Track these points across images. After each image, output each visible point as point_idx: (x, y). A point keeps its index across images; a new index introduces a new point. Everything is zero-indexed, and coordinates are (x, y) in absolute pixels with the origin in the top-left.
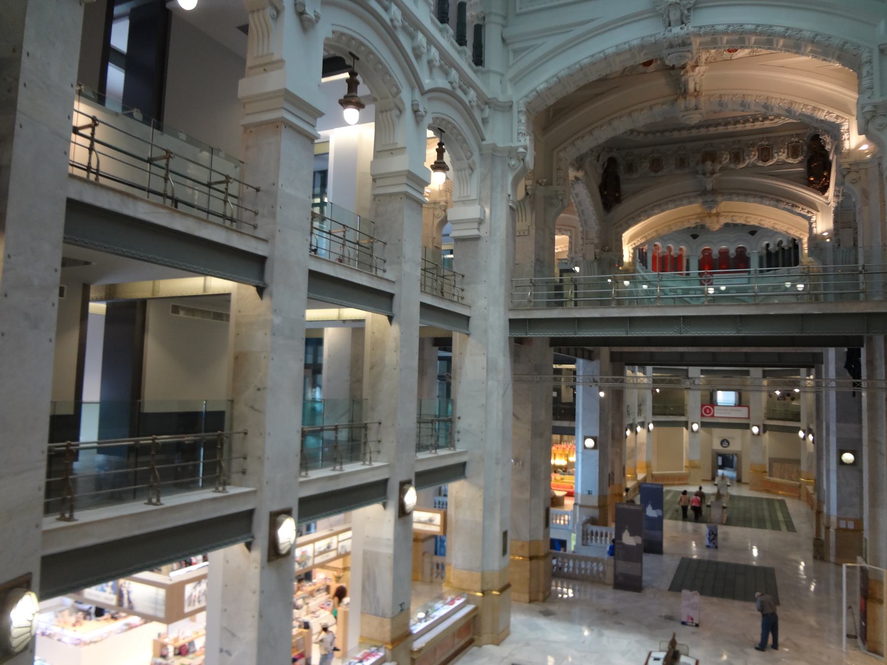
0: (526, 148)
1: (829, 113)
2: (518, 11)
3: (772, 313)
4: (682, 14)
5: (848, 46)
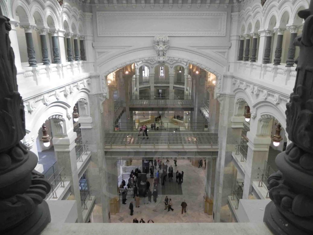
2: (99, 35)
4: (164, 53)
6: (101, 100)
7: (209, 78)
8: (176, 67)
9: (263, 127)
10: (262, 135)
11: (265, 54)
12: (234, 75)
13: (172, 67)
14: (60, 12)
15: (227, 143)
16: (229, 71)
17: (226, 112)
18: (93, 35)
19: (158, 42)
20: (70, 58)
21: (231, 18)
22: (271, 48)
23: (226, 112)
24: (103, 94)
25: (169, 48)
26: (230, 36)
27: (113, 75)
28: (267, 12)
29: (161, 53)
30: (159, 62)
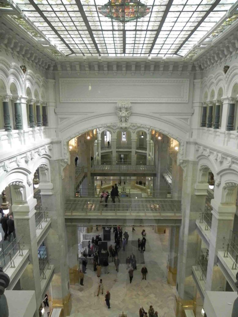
0: (67, 159)
3: (150, 218)
4: (126, 119)
6: (63, 166)
7: (172, 144)
8: (138, 132)
9: (227, 195)
10: (227, 204)
11: (228, 122)
12: (198, 141)
13: (134, 132)
14: (23, 79)
15: (191, 210)
16: (193, 137)
17: (190, 179)
18: (55, 101)
19: (120, 108)
20: (32, 124)
21: (194, 85)
22: (235, 115)
23: (190, 179)
24: (64, 160)
25: (132, 114)
26: (193, 103)
27: (75, 140)
28: (229, 79)
29: (123, 119)
30: (121, 128)
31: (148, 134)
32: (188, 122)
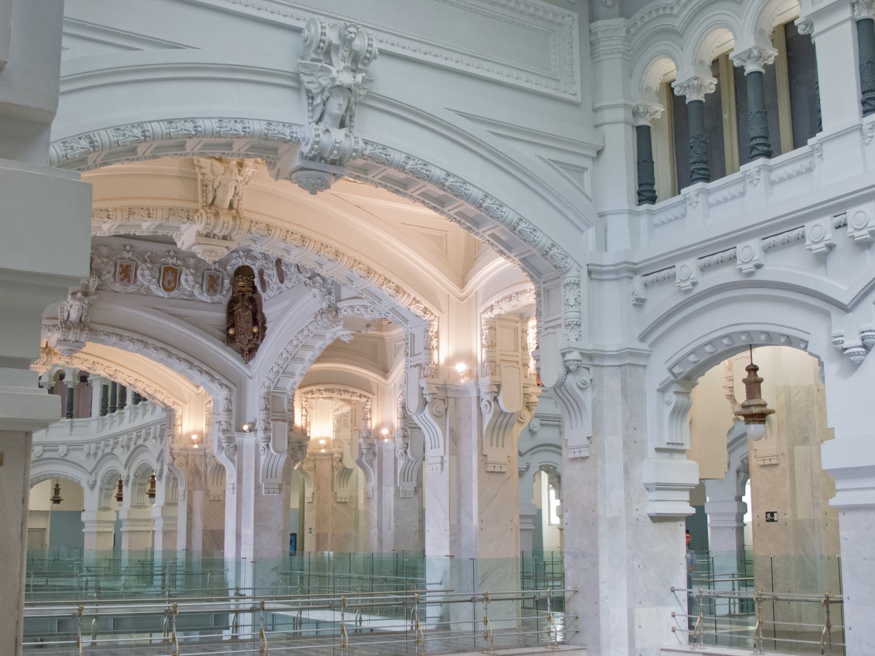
1: (414, 299)
4: (348, 108)
5: (555, 250)
7: (436, 352)
31: (92, 487)
32: (582, 182)
